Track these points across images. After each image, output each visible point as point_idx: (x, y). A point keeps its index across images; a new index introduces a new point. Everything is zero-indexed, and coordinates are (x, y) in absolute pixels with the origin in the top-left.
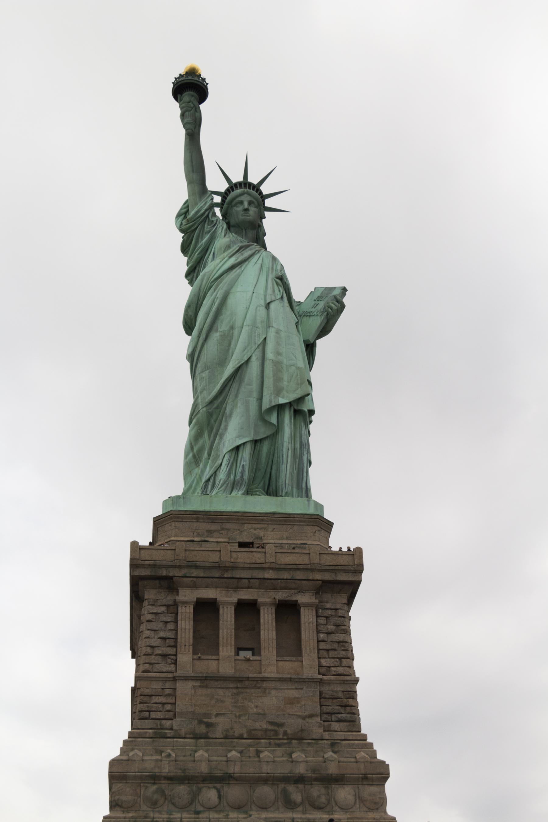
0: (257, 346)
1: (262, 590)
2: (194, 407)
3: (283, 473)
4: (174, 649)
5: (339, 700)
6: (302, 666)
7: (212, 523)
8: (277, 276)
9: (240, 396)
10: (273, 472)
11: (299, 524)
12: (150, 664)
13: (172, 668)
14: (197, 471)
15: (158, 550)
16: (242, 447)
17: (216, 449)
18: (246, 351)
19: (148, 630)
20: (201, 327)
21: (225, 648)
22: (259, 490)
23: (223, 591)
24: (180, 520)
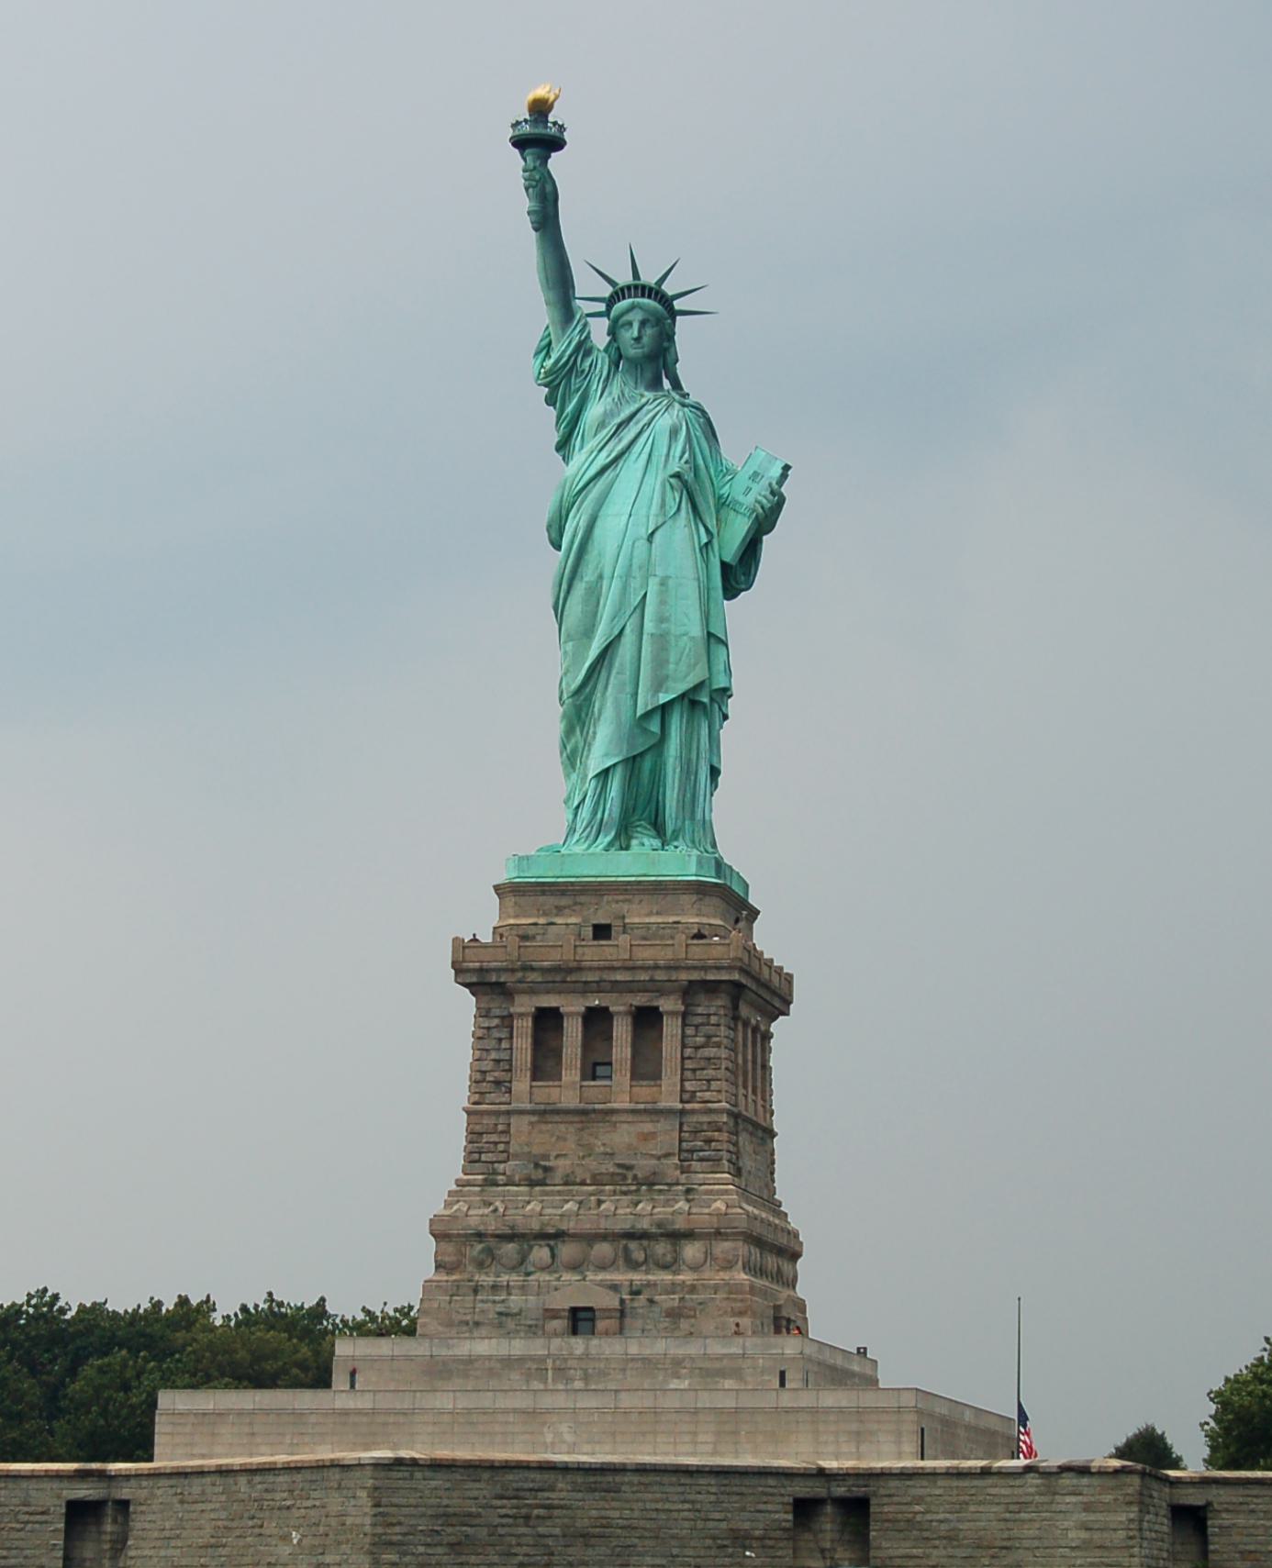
0: (632, 609)
4: (509, 1074)
5: (703, 1133)
8: (672, 472)
10: (660, 798)
13: (506, 1098)
14: (574, 776)
18: (616, 619)
21: (568, 1072)
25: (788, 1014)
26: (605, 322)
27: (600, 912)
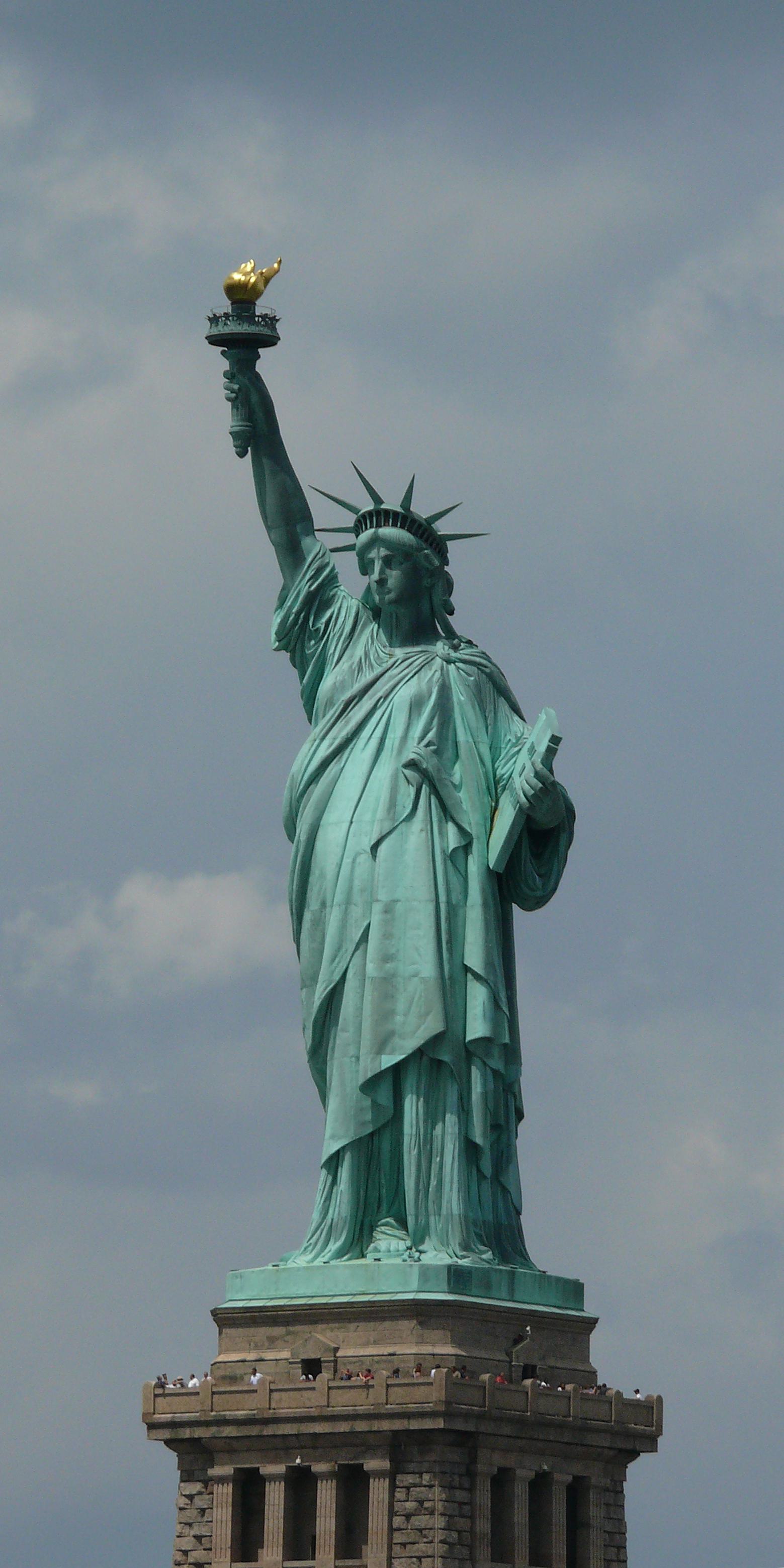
16: (341, 1154)
18: (337, 960)
22: (388, 1222)
25: (654, 1449)
26: (352, 557)
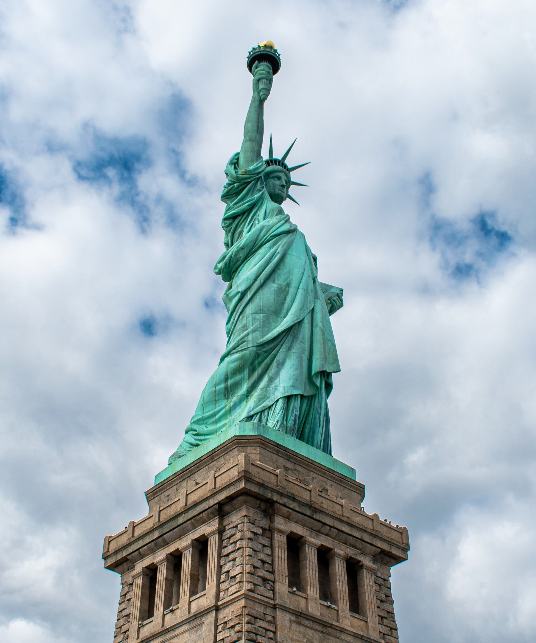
1: (337, 542)
2: (240, 342)
3: (319, 434)
6: (367, 627)
7: (287, 461)
9: (294, 350)
10: (307, 431)
11: (349, 488)
12: (255, 585)
13: (270, 594)
14: (224, 403)
15: (264, 471)
16: (294, 398)
17: (264, 390)
18: (302, 311)
19: (250, 548)
20: (259, 272)
23: (308, 531)
24: (264, 447)
27: (315, 481)
